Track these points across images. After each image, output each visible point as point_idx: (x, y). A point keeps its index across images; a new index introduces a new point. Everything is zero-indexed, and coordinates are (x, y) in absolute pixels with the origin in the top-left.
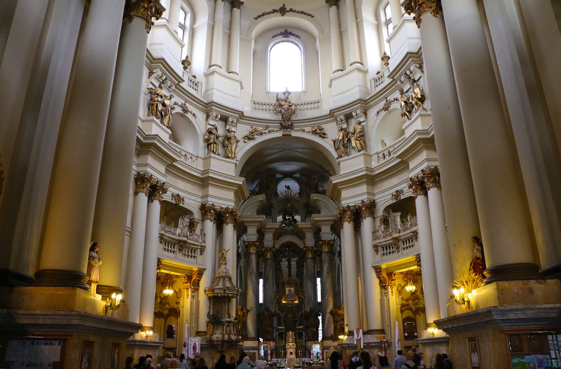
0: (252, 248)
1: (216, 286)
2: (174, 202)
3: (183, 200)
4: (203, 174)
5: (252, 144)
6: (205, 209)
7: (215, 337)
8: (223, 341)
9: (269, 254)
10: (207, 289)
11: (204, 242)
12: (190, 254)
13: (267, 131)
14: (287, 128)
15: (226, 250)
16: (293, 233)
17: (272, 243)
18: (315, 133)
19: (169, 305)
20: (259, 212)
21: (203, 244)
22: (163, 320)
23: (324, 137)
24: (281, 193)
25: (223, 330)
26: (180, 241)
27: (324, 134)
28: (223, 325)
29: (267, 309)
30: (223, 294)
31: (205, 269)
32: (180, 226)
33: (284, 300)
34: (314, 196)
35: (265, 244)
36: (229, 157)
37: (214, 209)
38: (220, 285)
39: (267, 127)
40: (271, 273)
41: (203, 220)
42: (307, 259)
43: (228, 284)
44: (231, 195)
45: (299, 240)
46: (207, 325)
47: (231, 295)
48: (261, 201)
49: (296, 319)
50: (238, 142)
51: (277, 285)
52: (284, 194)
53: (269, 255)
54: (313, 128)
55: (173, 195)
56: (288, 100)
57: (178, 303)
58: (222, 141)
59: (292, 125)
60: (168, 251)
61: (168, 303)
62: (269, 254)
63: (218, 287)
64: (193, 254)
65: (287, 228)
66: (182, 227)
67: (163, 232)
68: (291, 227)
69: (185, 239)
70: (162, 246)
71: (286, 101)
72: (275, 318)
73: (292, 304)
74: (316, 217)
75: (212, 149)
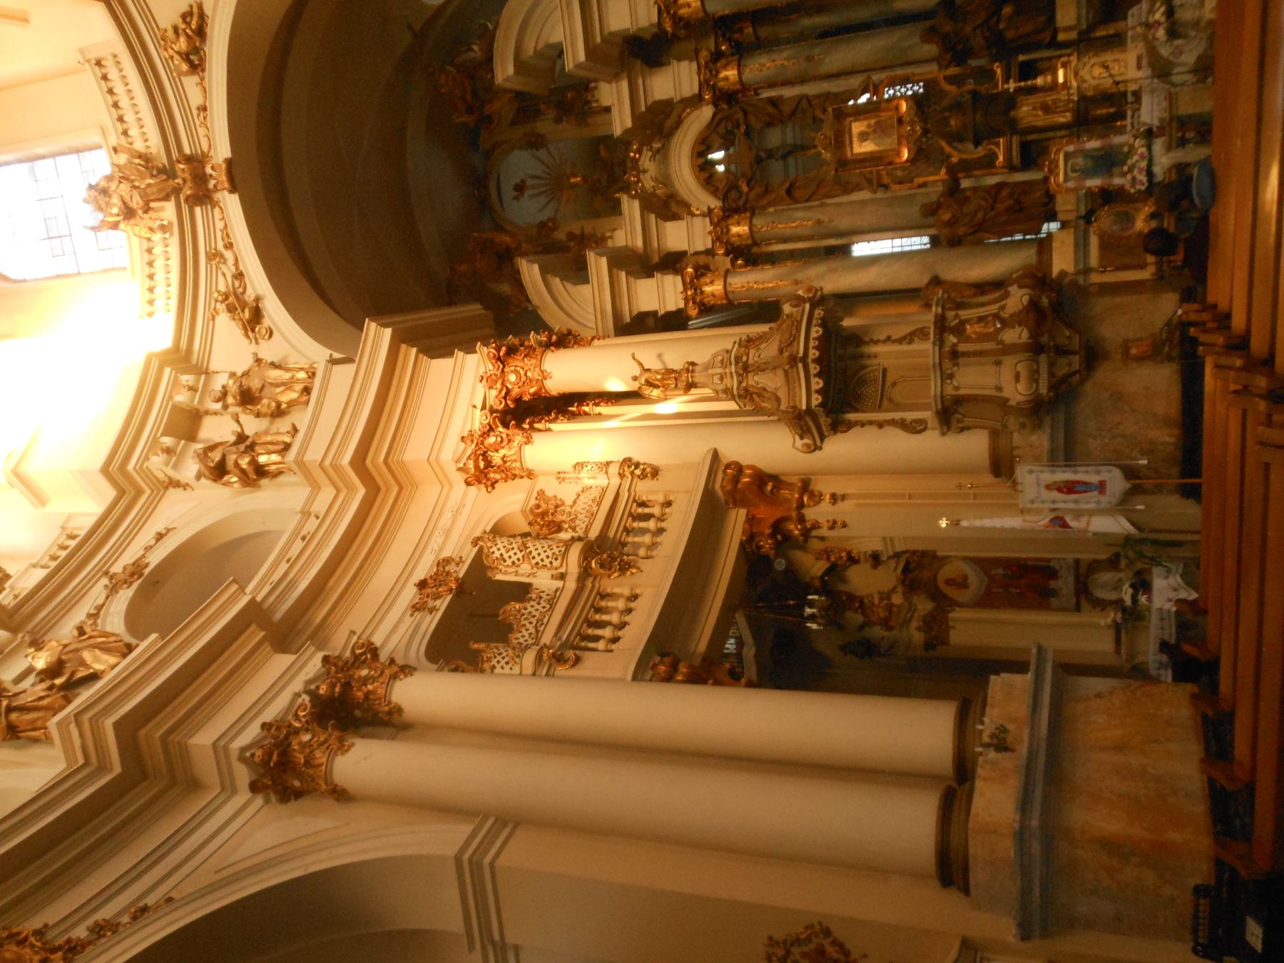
0: (708, 289)
1: (778, 400)
2: (443, 604)
3: (447, 561)
4: (351, 489)
5: (274, 310)
6: (484, 472)
7: (1017, 392)
8: (1035, 348)
9: (735, 229)
10: (799, 443)
11: (608, 463)
12: (651, 524)
13: (228, 255)
14: (200, 179)
15: (636, 371)
16: (662, 155)
17: (698, 222)
18: (195, 62)
19: (893, 590)
20: (579, 273)
21: (614, 470)
22: (957, 614)
23: (202, 16)
24: (541, 210)
25: (980, 353)
26: (585, 573)
27: (186, 16)
28: (955, 355)
29: (931, 210)
30: (814, 369)
31: (716, 455)
32: (522, 573)
33: (899, 154)
34: (504, 71)
35: (701, 248)
36: (307, 390)
37: (485, 434)
38: (770, 381)
39: (214, 256)
40: (800, 214)
41: (530, 474)
42: (744, 87)
43: (769, 351)
44: (440, 368)
45: (684, 126)
46: (962, 430)
47: (816, 332)
48: (544, 272)
49: (968, 97)
50: (258, 361)
51: (847, 189)
52: (543, 200)
53: (739, 229)
54: (180, 74)
55: (416, 608)
56: (104, 184)
57: (876, 559)
58: (262, 424)
59: (189, 159)
60: (622, 625)
61: (886, 596)
62: (735, 229)
63: (782, 394)
64: (656, 511)
65: (648, 175)
66: (525, 568)
67: (529, 657)
68: (646, 162)
69: (575, 553)
70: (590, 660)
71: (105, 192)
72: (965, 183)
73: (912, 123)
74: (576, 55)
75: (275, 457)
